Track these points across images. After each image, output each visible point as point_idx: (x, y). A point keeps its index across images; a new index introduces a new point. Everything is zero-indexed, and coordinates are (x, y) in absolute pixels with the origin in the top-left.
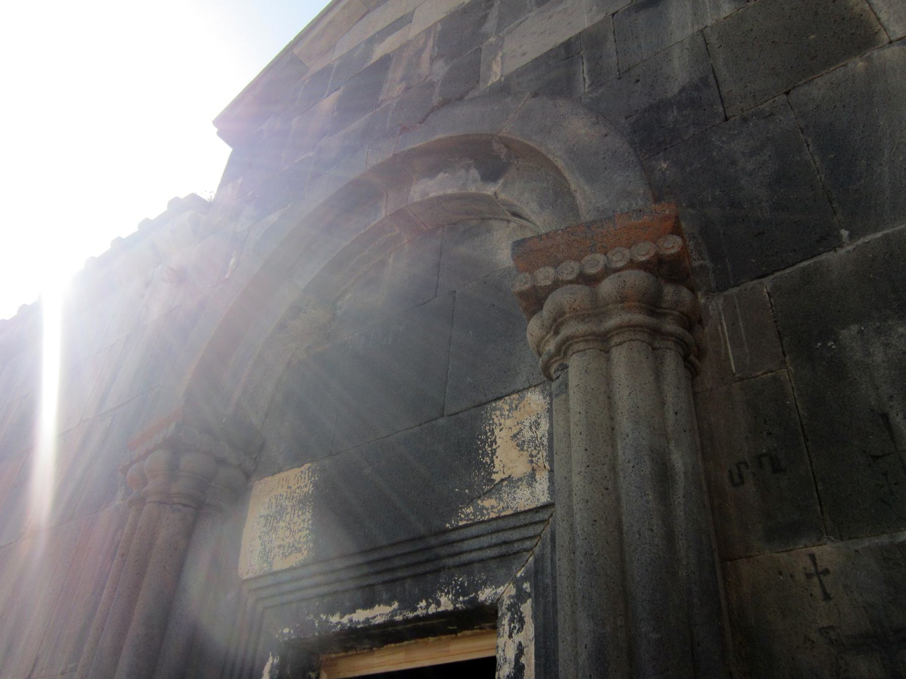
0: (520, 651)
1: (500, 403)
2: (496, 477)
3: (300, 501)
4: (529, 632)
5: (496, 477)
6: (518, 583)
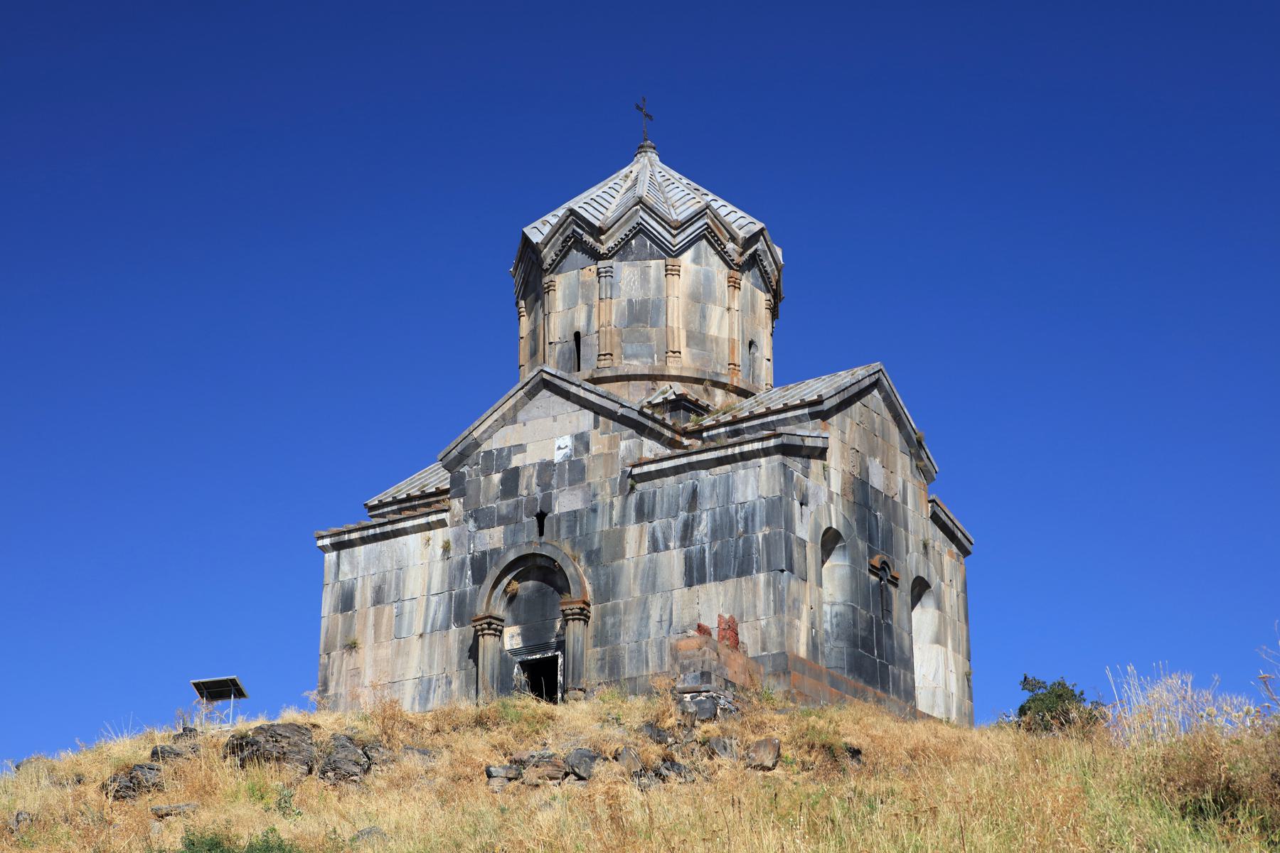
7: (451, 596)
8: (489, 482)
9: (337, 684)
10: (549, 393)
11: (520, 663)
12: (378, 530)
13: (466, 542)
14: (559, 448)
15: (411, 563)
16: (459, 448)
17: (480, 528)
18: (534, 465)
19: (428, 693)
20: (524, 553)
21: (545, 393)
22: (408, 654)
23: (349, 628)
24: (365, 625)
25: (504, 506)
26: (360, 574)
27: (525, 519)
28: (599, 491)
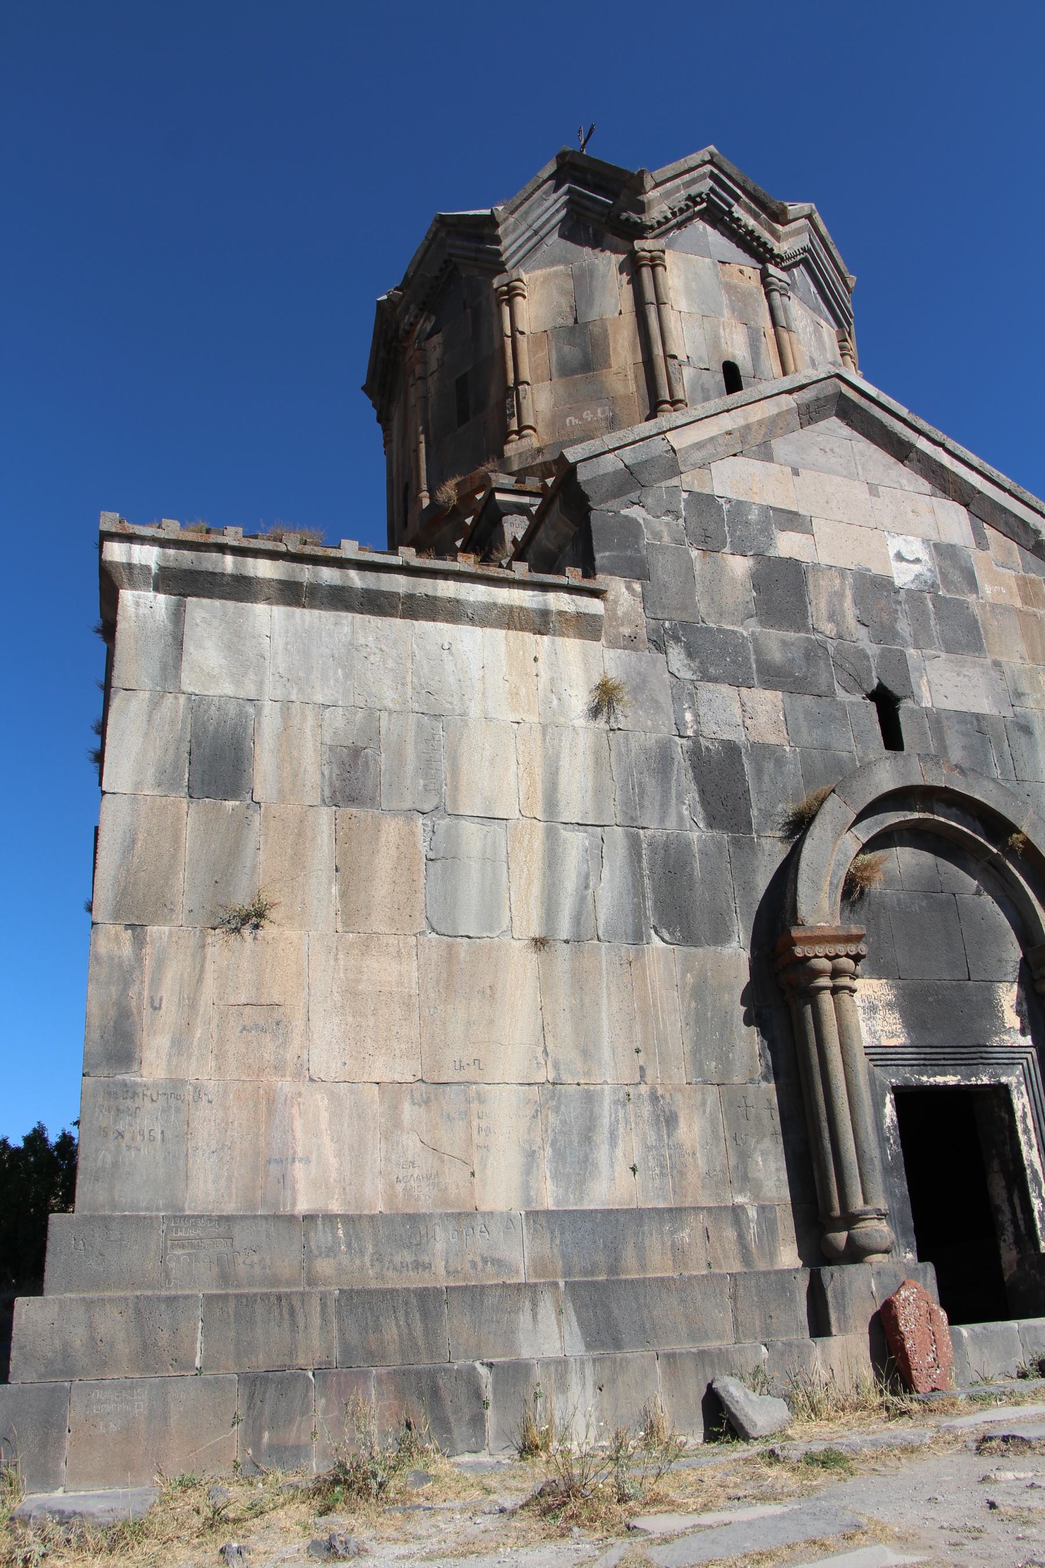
0: (1024, 1106)
1: (1001, 985)
2: (1008, 1026)
3: (888, 1005)
4: (1026, 1098)
5: (1008, 1026)
6: (1017, 1077)
7: (634, 845)
8: (719, 573)
9: (180, 1044)
10: (846, 431)
11: (896, 1090)
12: (356, 579)
13: (665, 699)
14: (900, 557)
15: (474, 710)
16: (628, 455)
17: (707, 678)
18: (842, 572)
19: (587, 1136)
20: (917, 780)
21: (834, 423)
22: (490, 994)
23: (224, 866)
24: (298, 860)
25: (777, 642)
26: (272, 690)
27: (841, 695)
28: (1025, 686)
